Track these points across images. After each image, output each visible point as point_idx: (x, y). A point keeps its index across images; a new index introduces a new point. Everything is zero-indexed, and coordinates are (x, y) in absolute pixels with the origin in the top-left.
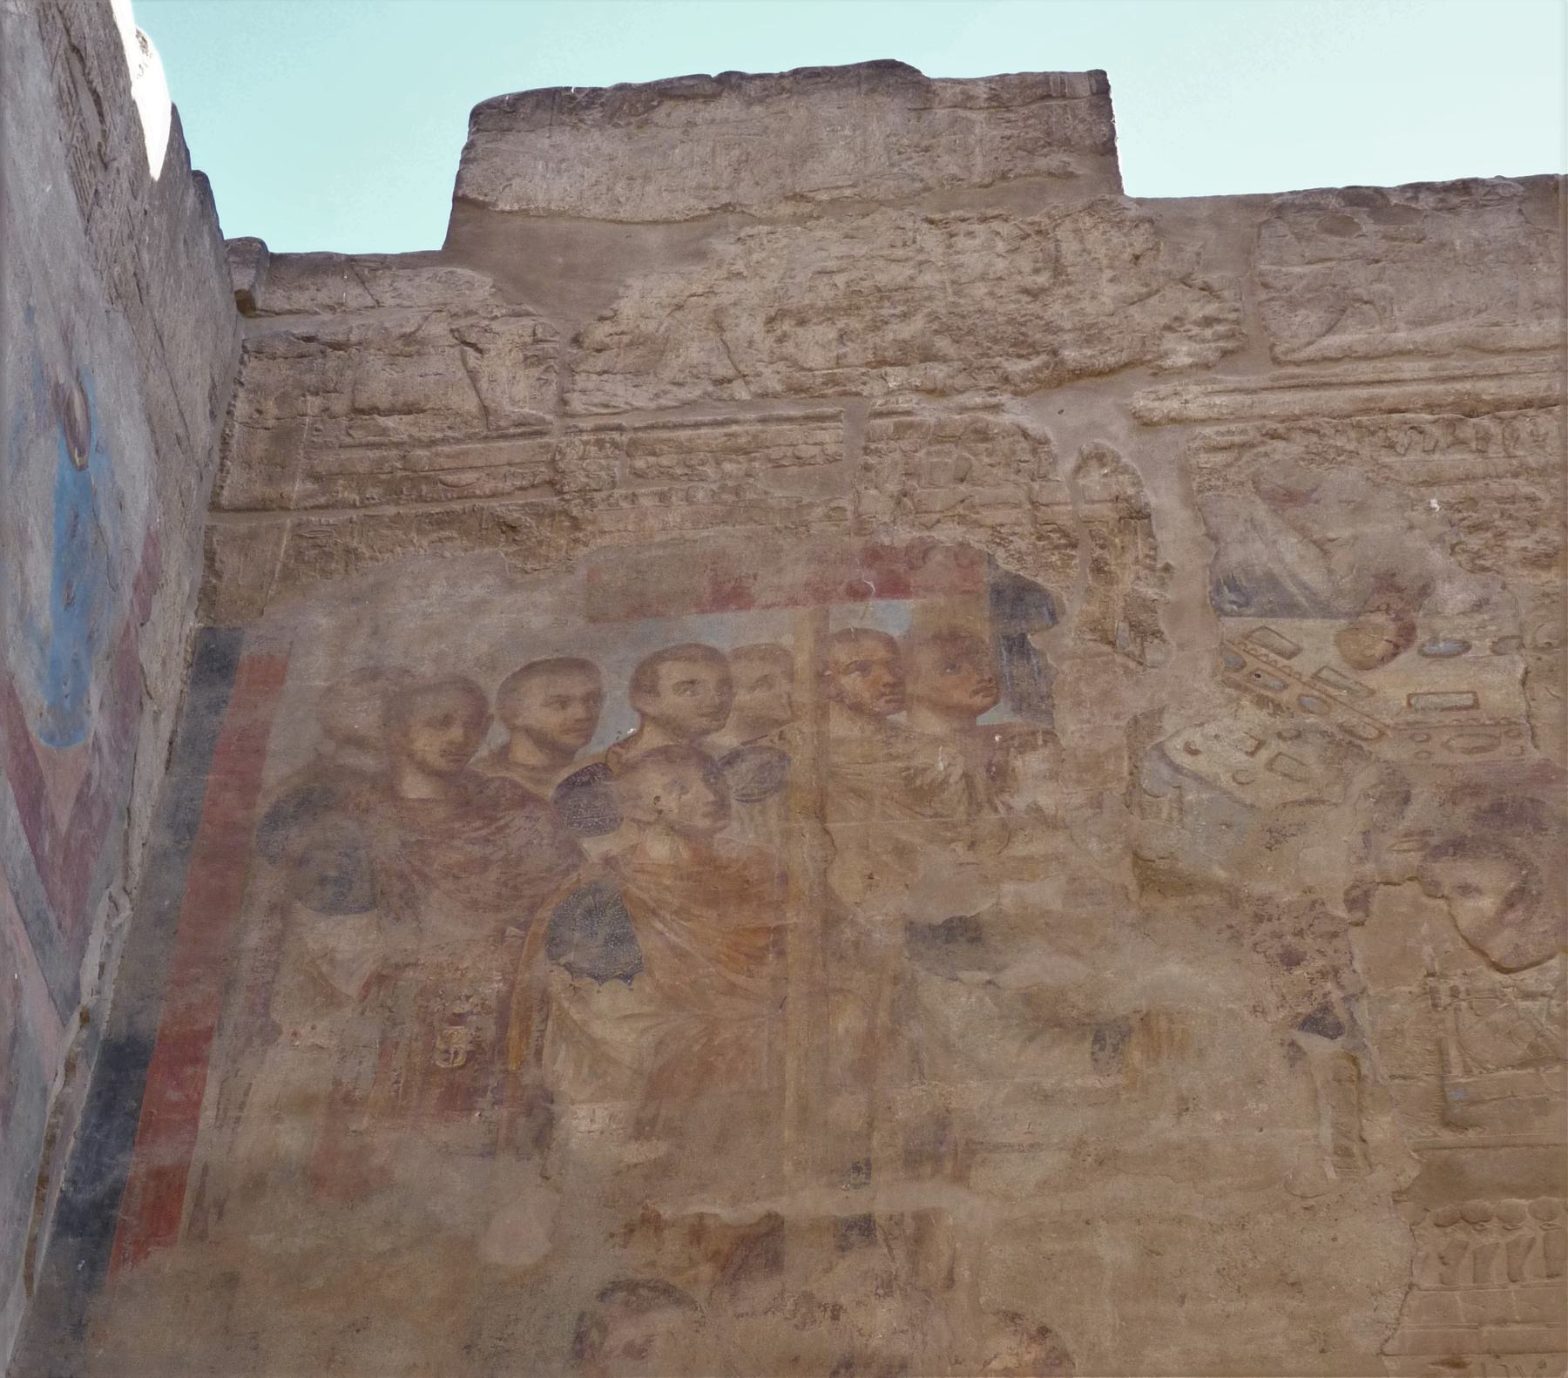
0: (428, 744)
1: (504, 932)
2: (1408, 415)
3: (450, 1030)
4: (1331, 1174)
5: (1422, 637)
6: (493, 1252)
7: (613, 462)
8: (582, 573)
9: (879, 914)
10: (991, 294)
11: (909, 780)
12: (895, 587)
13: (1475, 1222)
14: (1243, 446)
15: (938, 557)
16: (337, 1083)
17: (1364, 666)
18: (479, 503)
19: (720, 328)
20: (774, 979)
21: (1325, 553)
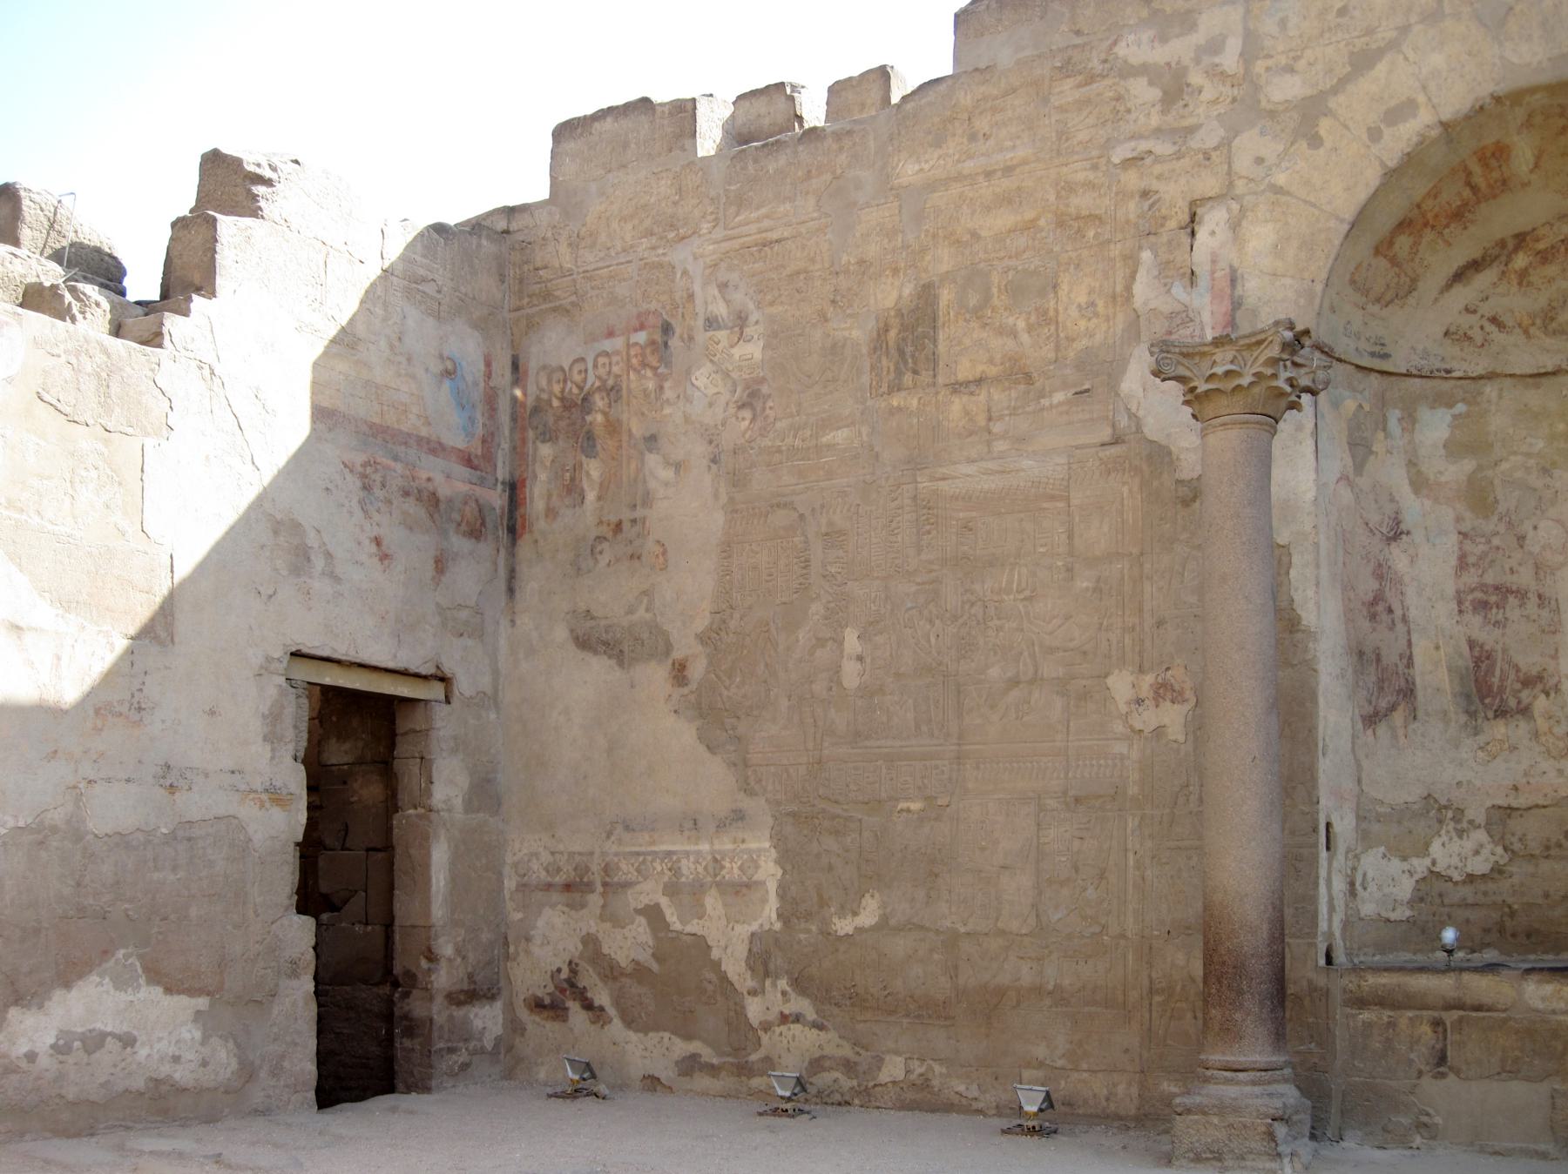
0: (557, 389)
12: (642, 327)
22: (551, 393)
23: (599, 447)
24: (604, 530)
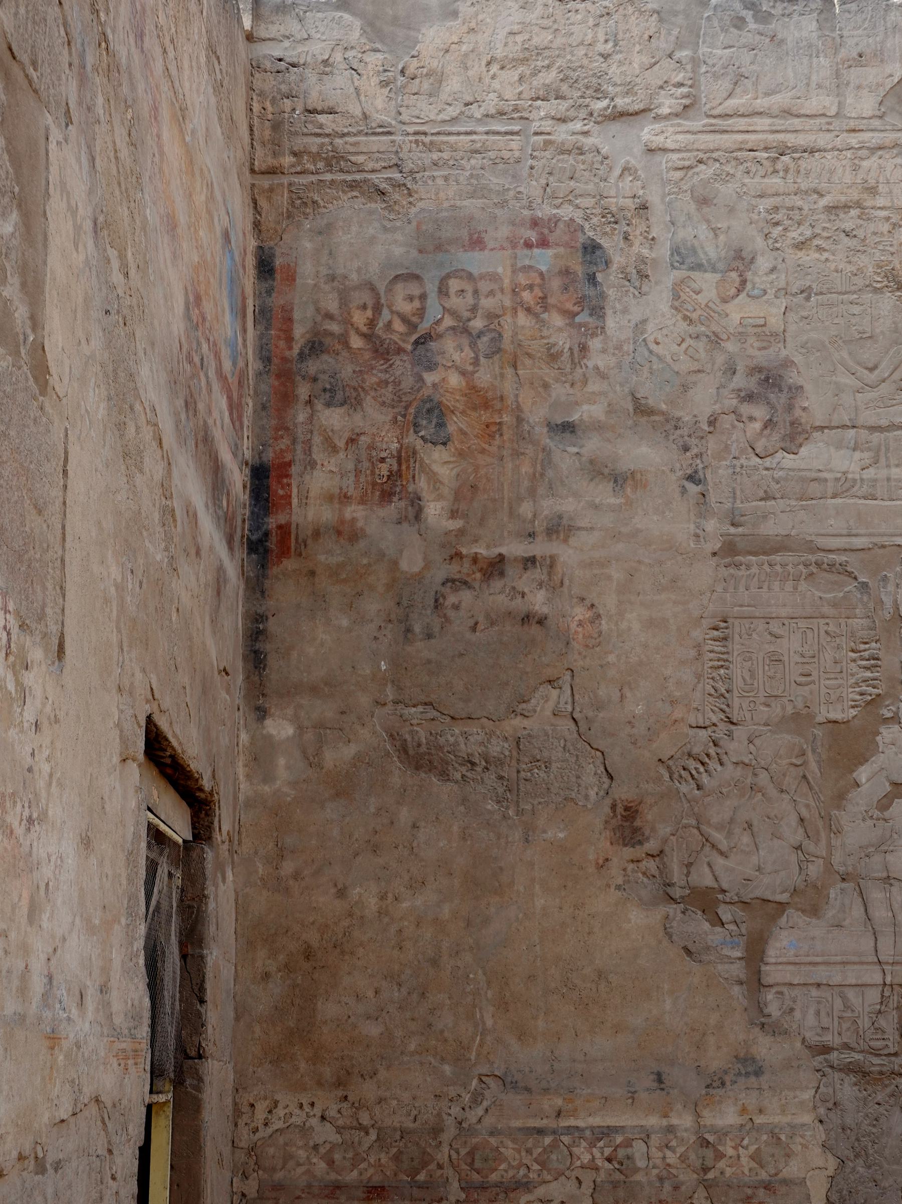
0: (360, 319)
3: (380, 465)
4: (692, 545)
5: (749, 286)
6: (404, 565)
7: (424, 155)
8: (414, 224)
9: (537, 415)
10: (586, 55)
11: (549, 349)
12: (544, 243)
13: (737, 566)
14: (690, 168)
15: (561, 225)
16: (341, 489)
17: (725, 301)
18: (369, 176)
19: (466, 68)
20: (499, 447)
21: (716, 235)
22: (347, 322)
23: (451, 428)
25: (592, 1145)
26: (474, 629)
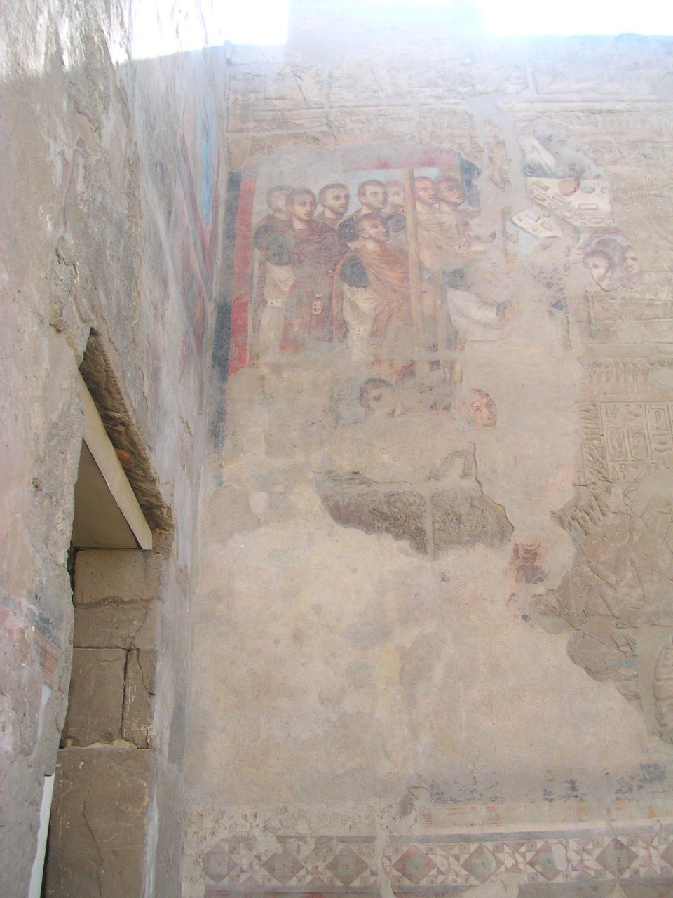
0: (301, 211)
1: (328, 272)
2: (576, 113)
13: (599, 365)
14: (531, 121)
23: (371, 277)
24: (383, 372)
25: (515, 851)
26: (392, 414)
